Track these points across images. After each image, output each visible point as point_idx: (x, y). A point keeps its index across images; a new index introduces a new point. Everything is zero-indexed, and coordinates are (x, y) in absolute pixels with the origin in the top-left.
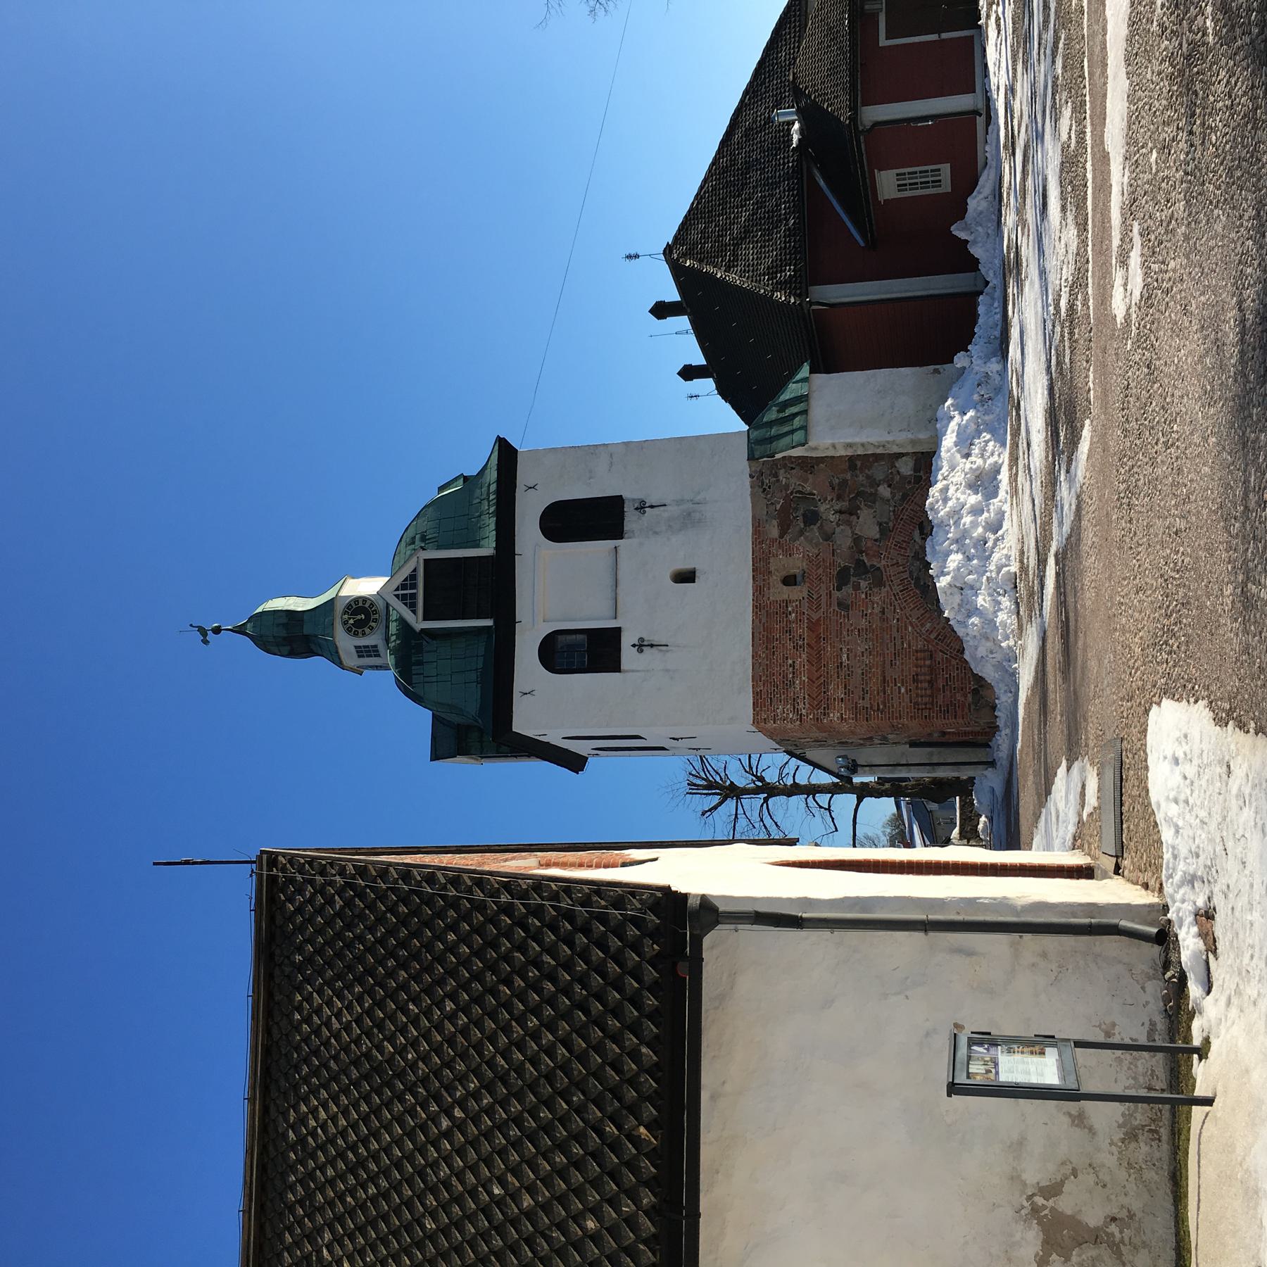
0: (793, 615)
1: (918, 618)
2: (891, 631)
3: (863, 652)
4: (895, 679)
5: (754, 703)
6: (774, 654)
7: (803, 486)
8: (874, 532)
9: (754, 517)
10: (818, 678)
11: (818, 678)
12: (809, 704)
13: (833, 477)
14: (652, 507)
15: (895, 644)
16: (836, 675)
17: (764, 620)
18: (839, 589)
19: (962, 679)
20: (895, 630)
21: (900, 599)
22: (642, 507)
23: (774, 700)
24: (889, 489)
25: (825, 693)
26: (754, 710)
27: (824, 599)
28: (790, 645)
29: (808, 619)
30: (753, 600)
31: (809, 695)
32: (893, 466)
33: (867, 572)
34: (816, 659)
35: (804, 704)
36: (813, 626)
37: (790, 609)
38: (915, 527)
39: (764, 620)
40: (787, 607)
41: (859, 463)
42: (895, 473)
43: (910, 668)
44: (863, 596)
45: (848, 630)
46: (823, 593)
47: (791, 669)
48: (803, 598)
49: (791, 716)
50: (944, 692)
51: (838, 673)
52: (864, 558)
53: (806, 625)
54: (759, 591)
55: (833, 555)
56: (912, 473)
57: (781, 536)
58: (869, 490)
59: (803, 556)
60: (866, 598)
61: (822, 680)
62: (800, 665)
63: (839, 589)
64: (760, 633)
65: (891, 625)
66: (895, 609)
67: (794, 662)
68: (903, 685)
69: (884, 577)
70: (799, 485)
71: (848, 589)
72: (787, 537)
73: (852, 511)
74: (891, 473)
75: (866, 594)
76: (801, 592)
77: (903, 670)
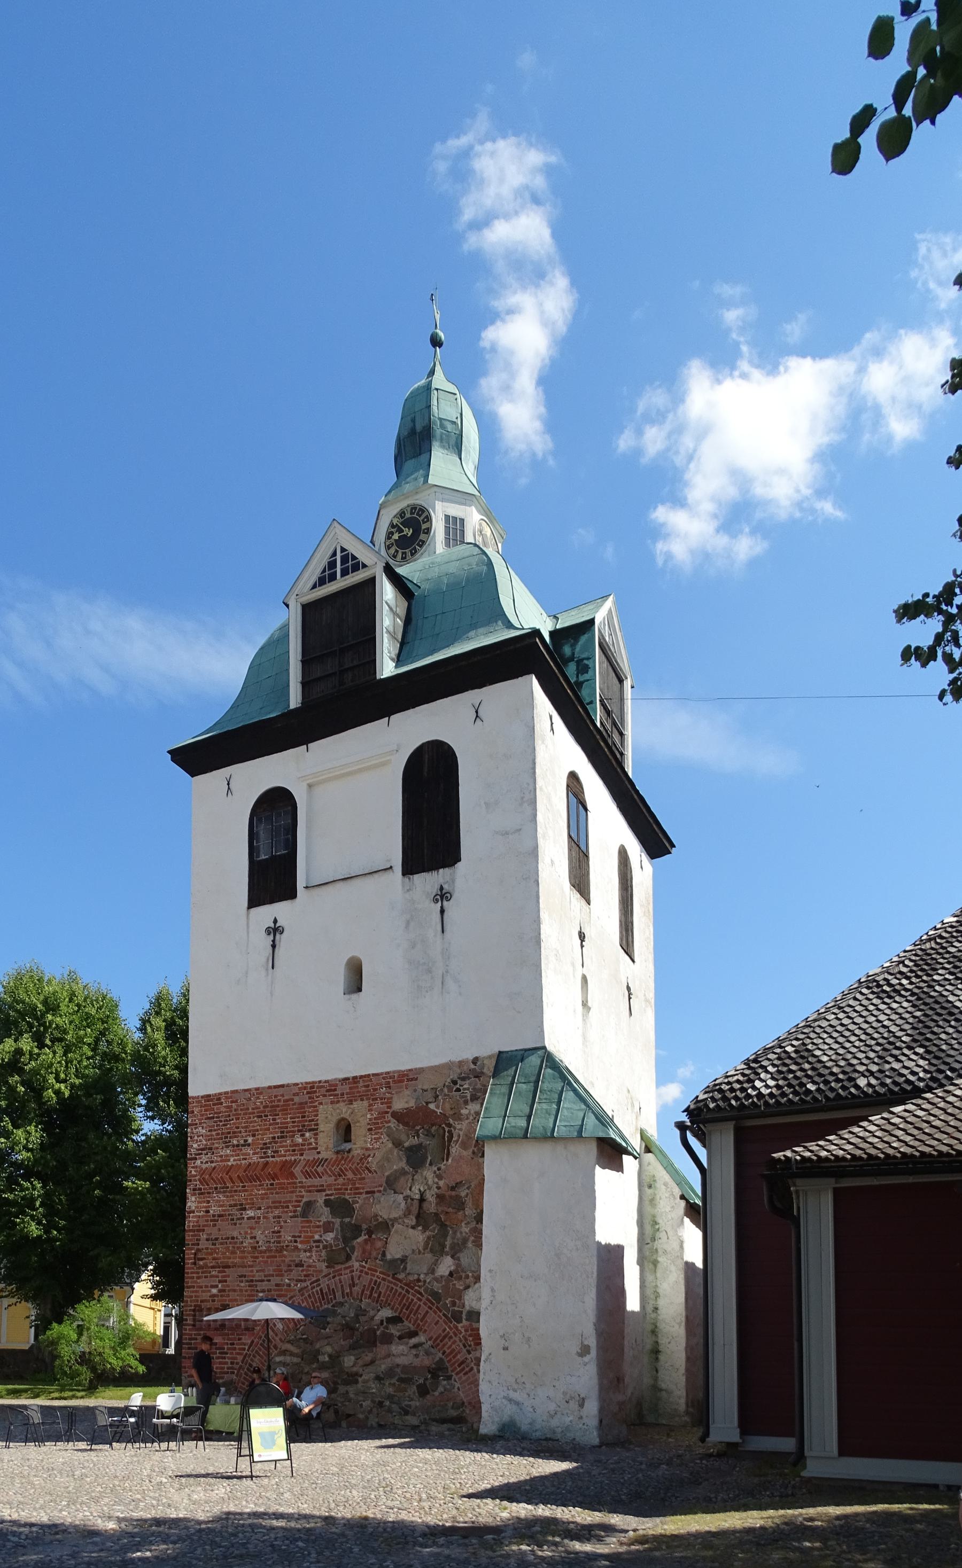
0: (300, 1140)
3: (255, 1238)
4: (226, 1281)
7: (457, 1141)
8: (394, 1252)
9: (421, 1070)
10: (231, 1179)
11: (231, 1179)
12: (207, 1168)
13: (468, 1188)
14: (442, 911)
15: (262, 1281)
16: (232, 1203)
17: (297, 1099)
23: (211, 1123)
24: (447, 1273)
26: (202, 1097)
28: (267, 1138)
29: (295, 1160)
30: (320, 1082)
31: (215, 1168)
34: (251, 1175)
35: (207, 1162)
36: (286, 1168)
37: (307, 1135)
38: (395, 1312)
39: (297, 1099)
44: (317, 1237)
45: (279, 1217)
47: (242, 1142)
48: (319, 1153)
49: (195, 1146)
51: (235, 1205)
54: (330, 1089)
56: (467, 1308)
57: (395, 1115)
59: (367, 1149)
63: (327, 1203)
64: (283, 1096)
65: (282, 1275)
66: (301, 1281)
67: (249, 1145)
68: (220, 1291)
71: (325, 1214)
72: (393, 1124)
73: (422, 1220)
74: (467, 1277)
75: (318, 1241)
77: (235, 1291)
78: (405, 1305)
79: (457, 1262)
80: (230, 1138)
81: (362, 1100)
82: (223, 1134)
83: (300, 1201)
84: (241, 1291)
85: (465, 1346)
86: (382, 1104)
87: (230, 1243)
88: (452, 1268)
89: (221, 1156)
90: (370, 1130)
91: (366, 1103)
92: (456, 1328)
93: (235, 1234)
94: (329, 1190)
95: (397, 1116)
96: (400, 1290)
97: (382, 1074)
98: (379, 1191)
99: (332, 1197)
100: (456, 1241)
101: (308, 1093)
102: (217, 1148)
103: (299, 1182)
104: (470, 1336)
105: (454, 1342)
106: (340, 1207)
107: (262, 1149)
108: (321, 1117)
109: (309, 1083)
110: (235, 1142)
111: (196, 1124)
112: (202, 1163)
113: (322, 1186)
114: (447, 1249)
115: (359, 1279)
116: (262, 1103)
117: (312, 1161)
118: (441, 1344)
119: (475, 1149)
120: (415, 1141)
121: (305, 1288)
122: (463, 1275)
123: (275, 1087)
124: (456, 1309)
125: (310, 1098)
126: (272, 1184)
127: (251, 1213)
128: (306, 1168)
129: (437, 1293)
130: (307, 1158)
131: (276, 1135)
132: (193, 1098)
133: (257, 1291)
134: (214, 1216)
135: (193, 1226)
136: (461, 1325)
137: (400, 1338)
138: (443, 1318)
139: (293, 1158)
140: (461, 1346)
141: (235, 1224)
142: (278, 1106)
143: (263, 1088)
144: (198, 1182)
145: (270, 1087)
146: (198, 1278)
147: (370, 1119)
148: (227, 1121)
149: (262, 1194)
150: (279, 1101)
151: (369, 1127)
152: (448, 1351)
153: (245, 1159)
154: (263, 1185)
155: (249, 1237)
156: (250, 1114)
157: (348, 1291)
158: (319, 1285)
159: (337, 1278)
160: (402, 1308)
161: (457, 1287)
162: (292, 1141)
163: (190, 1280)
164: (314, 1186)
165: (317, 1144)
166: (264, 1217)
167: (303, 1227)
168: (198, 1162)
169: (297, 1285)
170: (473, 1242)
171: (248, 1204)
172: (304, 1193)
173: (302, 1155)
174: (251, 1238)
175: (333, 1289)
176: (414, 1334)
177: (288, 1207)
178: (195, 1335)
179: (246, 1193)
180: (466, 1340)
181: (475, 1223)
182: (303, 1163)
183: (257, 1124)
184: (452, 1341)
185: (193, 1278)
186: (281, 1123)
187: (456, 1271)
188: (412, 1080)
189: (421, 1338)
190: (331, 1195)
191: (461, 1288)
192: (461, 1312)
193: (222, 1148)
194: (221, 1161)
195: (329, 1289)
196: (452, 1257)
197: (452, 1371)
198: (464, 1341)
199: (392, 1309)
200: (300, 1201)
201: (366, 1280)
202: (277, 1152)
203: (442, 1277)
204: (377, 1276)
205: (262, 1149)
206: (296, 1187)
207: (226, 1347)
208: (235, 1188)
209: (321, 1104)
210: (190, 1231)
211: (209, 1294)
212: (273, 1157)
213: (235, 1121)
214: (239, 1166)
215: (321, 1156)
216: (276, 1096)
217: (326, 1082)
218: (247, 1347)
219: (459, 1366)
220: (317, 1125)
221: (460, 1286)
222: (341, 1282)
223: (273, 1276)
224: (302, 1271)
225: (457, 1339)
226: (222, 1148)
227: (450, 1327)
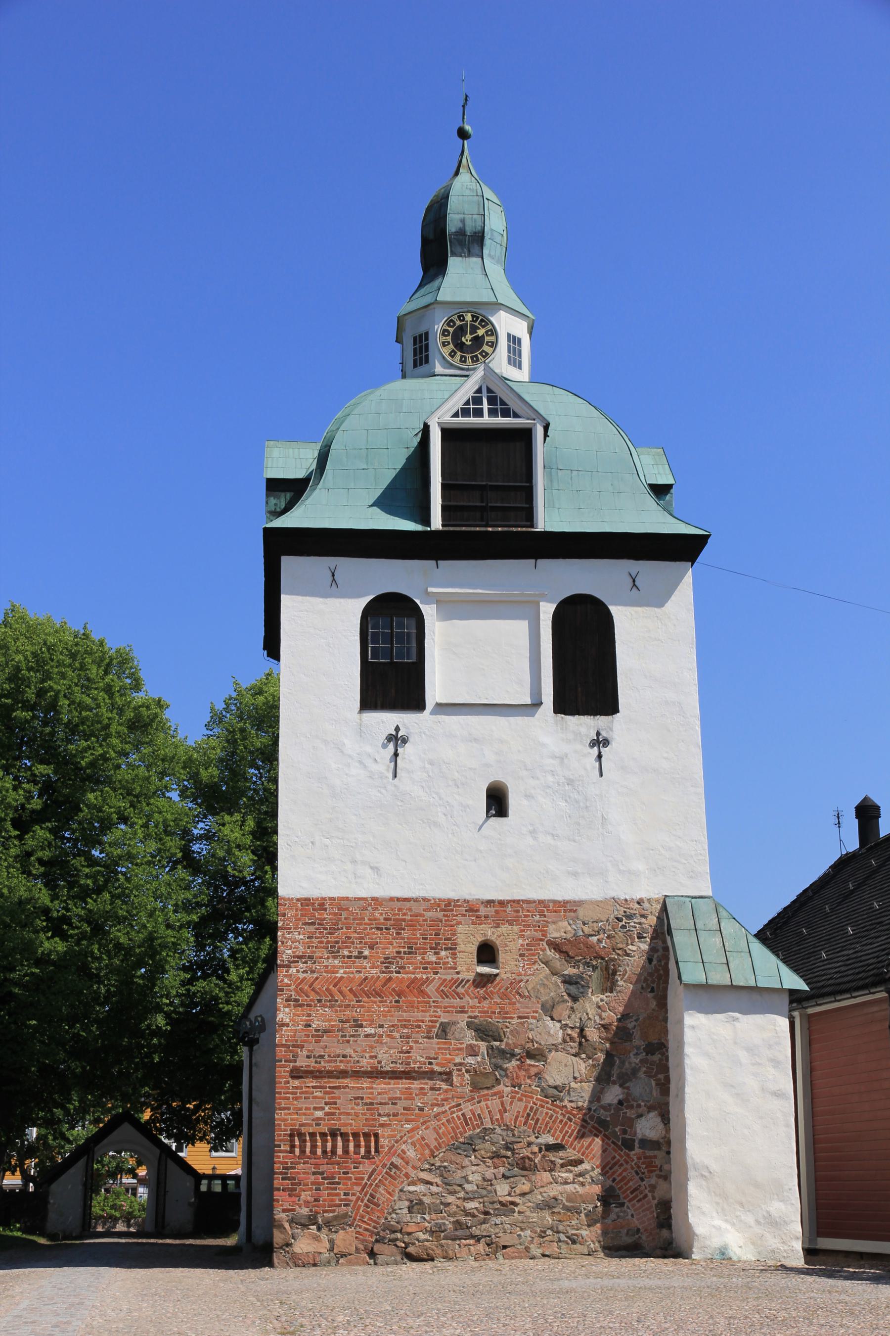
0: (433, 958)
1: (423, 1139)
2: (406, 1099)
4: (335, 1103)
5: (308, 899)
6: (378, 929)
7: (624, 975)
9: (579, 903)
10: (341, 992)
11: (341, 992)
12: (305, 978)
13: (636, 1020)
14: (600, 756)
15: (385, 1104)
17: (429, 914)
18: (469, 1025)
19: (332, 1200)
20: (407, 1103)
21: (454, 1112)
22: (600, 742)
23: (312, 929)
24: (616, 1101)
25: (319, 1001)
26: (298, 900)
27: (457, 1002)
28: (391, 951)
29: (427, 978)
30: (458, 901)
31: (317, 978)
32: (650, 1109)
33: (497, 1067)
36: (417, 987)
37: (443, 953)
38: (557, 1139)
39: (429, 914)
40: (446, 949)
41: (656, 1057)
42: (640, 1111)
43: (351, 1125)
46: (469, 1001)
48: (458, 973)
49: (289, 952)
50: (314, 1173)
51: (347, 1021)
52: (514, 1063)
53: (418, 976)
54: (472, 909)
55: (519, 1018)
56: (639, 1136)
58: (615, 1072)
59: (519, 974)
60: (455, 1065)
61: (338, 997)
62: (361, 967)
64: (410, 910)
66: (438, 1105)
67: (365, 957)
68: (327, 1114)
69: (486, 1092)
70: (626, 971)
71: (469, 1038)
72: (550, 954)
74: (639, 1106)
75: (461, 1064)
76: (468, 970)
77: (348, 1114)
78: (567, 1132)
79: (626, 1091)
80: (339, 948)
81: (511, 924)
82: (328, 942)
83: (436, 1022)
84: (356, 1115)
85: (637, 1173)
86: (536, 931)
87: (341, 1061)
88: (621, 1097)
89: (327, 967)
90: (521, 955)
91: (516, 928)
92: (628, 1155)
93: (349, 1051)
94: (472, 1012)
95: (555, 946)
96: (560, 1117)
97: (534, 902)
98: (534, 1017)
99: (476, 1021)
100: (624, 1070)
101: (442, 910)
102: (321, 958)
103: (434, 1002)
104: (643, 1163)
105: (625, 1170)
106: (484, 1032)
107: (382, 963)
108: (460, 938)
109: (444, 900)
110: (346, 953)
111: (290, 929)
112: (298, 971)
113: (464, 1007)
114: (614, 1078)
115: (511, 1103)
116: (381, 914)
117: (450, 981)
118: (611, 1172)
119: (644, 985)
120: (574, 971)
121: (443, 1112)
122: (635, 1104)
123: (398, 899)
124: (627, 1136)
125: (445, 916)
126: (397, 1002)
127: (369, 1030)
128: (442, 988)
129: (605, 1121)
130: (443, 977)
131: (402, 950)
132: (284, 899)
133: (380, 1115)
134: (317, 1031)
135: (286, 1041)
136: (633, 1152)
137: (562, 1166)
138: (613, 1145)
139: (424, 977)
140: (634, 1173)
141: (348, 1042)
142: (404, 920)
143: (384, 900)
144: (293, 993)
145: (392, 899)
146: (296, 1099)
147: (522, 945)
148: (334, 929)
149: (384, 1011)
150: (405, 914)
151: (521, 952)
152: (618, 1179)
153: (360, 972)
154: (386, 1001)
155: (367, 1055)
156: (365, 924)
157: (499, 1117)
158: (461, 1110)
159: (483, 1103)
160: (565, 1136)
161: (628, 1115)
162: (423, 958)
163: (283, 1102)
164: (453, 1007)
165: (455, 963)
166: (388, 1036)
167: (439, 1049)
168: (293, 970)
169: (433, 1109)
170: (645, 1073)
171: (366, 1020)
172: (440, 1013)
173: (436, 973)
174: (371, 1057)
175: (479, 1115)
176: (581, 1162)
177: (419, 1027)
178: (292, 1163)
179: (362, 1010)
180: (639, 1167)
181: (644, 1054)
182: (436, 984)
183: (376, 936)
184: (623, 1168)
185: (288, 1099)
186: (408, 938)
187: (627, 1100)
188: (571, 911)
189: (586, 1166)
190: (475, 1017)
191: (633, 1116)
192: (634, 1141)
193: (328, 958)
194: (326, 972)
195: (473, 1114)
196: (621, 1086)
197: (625, 1198)
198: (636, 1169)
199: (553, 1136)
200: (436, 1022)
201: (519, 1106)
202: (403, 968)
203: (610, 1105)
204: (534, 1103)
205: (382, 963)
206: (430, 1007)
207: (337, 1176)
208: (347, 1002)
209: (459, 923)
210: (283, 1046)
211: (311, 1117)
212: (397, 972)
213: (344, 930)
214: (351, 980)
215: (461, 976)
216: (400, 910)
217: (465, 901)
218: (366, 1177)
219: (632, 1193)
220: (456, 944)
221: (631, 1113)
222: (488, 1108)
223: (400, 1099)
224: (438, 1095)
225: (629, 1167)
226: (328, 958)
227: (620, 1155)
